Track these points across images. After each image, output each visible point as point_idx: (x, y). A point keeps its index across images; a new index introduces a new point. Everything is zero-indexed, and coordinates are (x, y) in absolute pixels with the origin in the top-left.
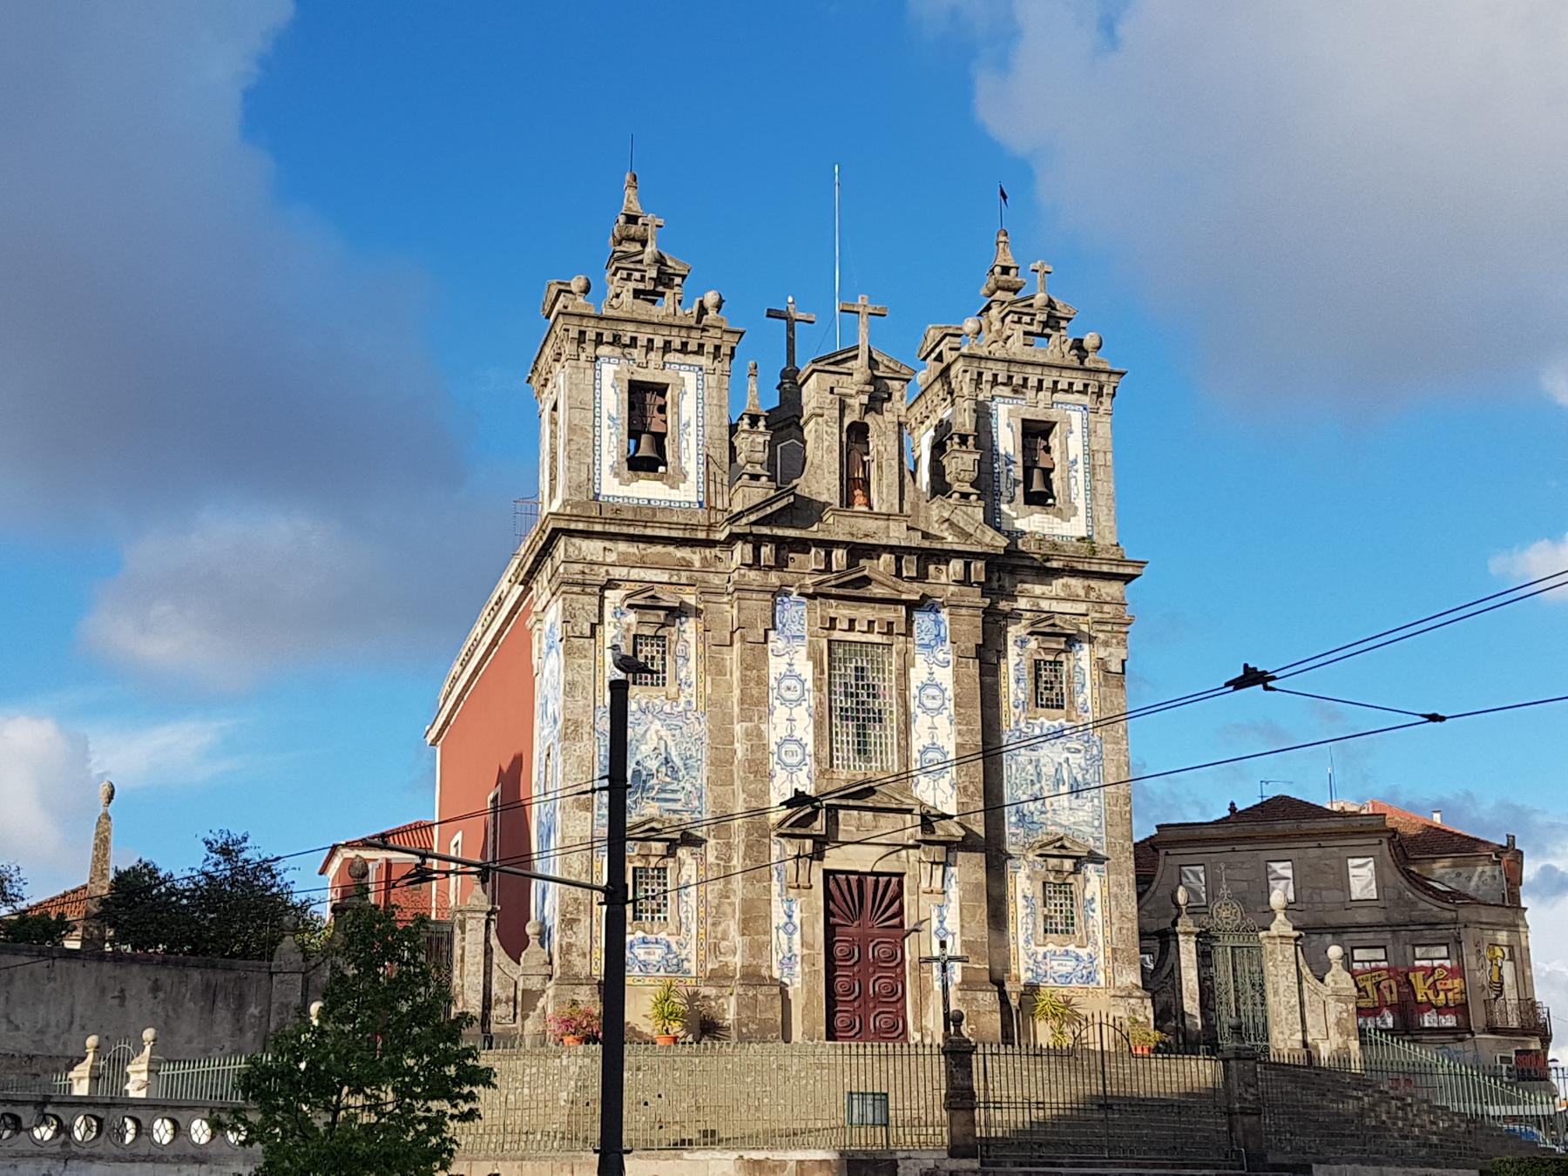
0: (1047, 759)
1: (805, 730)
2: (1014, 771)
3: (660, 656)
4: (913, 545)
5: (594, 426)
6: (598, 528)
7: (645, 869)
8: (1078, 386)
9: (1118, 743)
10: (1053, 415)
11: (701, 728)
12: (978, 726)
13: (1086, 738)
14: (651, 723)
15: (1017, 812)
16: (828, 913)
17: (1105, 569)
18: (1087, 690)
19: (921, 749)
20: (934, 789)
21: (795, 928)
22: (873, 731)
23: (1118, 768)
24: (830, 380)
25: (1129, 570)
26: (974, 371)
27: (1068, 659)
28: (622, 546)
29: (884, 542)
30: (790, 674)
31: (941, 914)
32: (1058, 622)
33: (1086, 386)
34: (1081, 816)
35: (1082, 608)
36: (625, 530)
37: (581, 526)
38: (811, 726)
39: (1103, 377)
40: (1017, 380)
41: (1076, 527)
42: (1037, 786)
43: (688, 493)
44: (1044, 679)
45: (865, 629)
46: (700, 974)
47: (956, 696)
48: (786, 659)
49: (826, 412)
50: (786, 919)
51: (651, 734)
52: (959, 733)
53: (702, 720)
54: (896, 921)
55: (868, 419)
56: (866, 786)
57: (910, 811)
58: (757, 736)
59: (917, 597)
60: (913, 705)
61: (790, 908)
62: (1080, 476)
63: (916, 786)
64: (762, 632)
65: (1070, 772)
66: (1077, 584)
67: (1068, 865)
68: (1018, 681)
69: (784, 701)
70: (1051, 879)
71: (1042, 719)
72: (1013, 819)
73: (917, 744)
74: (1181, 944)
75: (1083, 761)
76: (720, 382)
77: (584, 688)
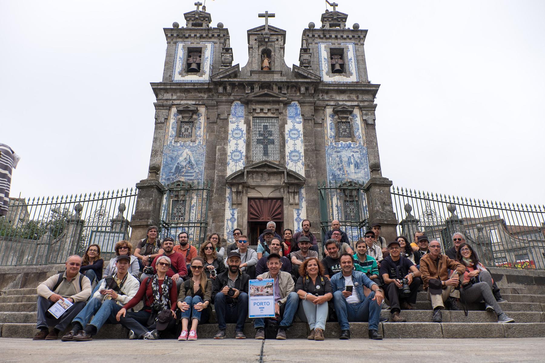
0: (344, 155)
1: (242, 147)
2: (330, 160)
3: (190, 128)
4: (283, 81)
5: (174, 61)
6: (168, 87)
7: (178, 201)
8: (350, 36)
9: (374, 148)
10: (342, 46)
11: (203, 150)
12: (313, 143)
13: (360, 147)
14: (185, 150)
15: (332, 175)
16: (250, 213)
17: (363, 88)
18: (360, 131)
19: (290, 152)
20: (295, 166)
21: (235, 220)
22: (270, 147)
23: (375, 157)
24: (256, 37)
25: (374, 88)
26: (311, 35)
27: (351, 121)
28: (178, 94)
29: (272, 80)
30: (238, 129)
31: (298, 212)
32: (345, 107)
33: (353, 37)
34: (360, 175)
35: (356, 103)
36: (178, 87)
37: (162, 87)
38: (245, 146)
39: (359, 33)
40: (328, 36)
41: (353, 79)
42: (341, 165)
43: (206, 78)
44: (343, 127)
45: (267, 111)
46: (196, 240)
47: (304, 133)
48: (236, 124)
49: (253, 46)
50: (231, 216)
51: (185, 153)
52: (306, 146)
53: (204, 148)
54: (279, 216)
55: (270, 48)
56: (264, 163)
57: (283, 172)
58: (223, 150)
59: (286, 99)
60: (286, 137)
61: (233, 212)
62: (353, 64)
63: (288, 165)
64: (226, 115)
65: (354, 160)
66: (354, 97)
67: (354, 193)
68: (331, 129)
69: (234, 138)
70: (348, 199)
71: (341, 142)
72: (331, 177)
73: (288, 150)
74: (410, 226)
75: (359, 156)
76: (219, 46)
77: (160, 139)
